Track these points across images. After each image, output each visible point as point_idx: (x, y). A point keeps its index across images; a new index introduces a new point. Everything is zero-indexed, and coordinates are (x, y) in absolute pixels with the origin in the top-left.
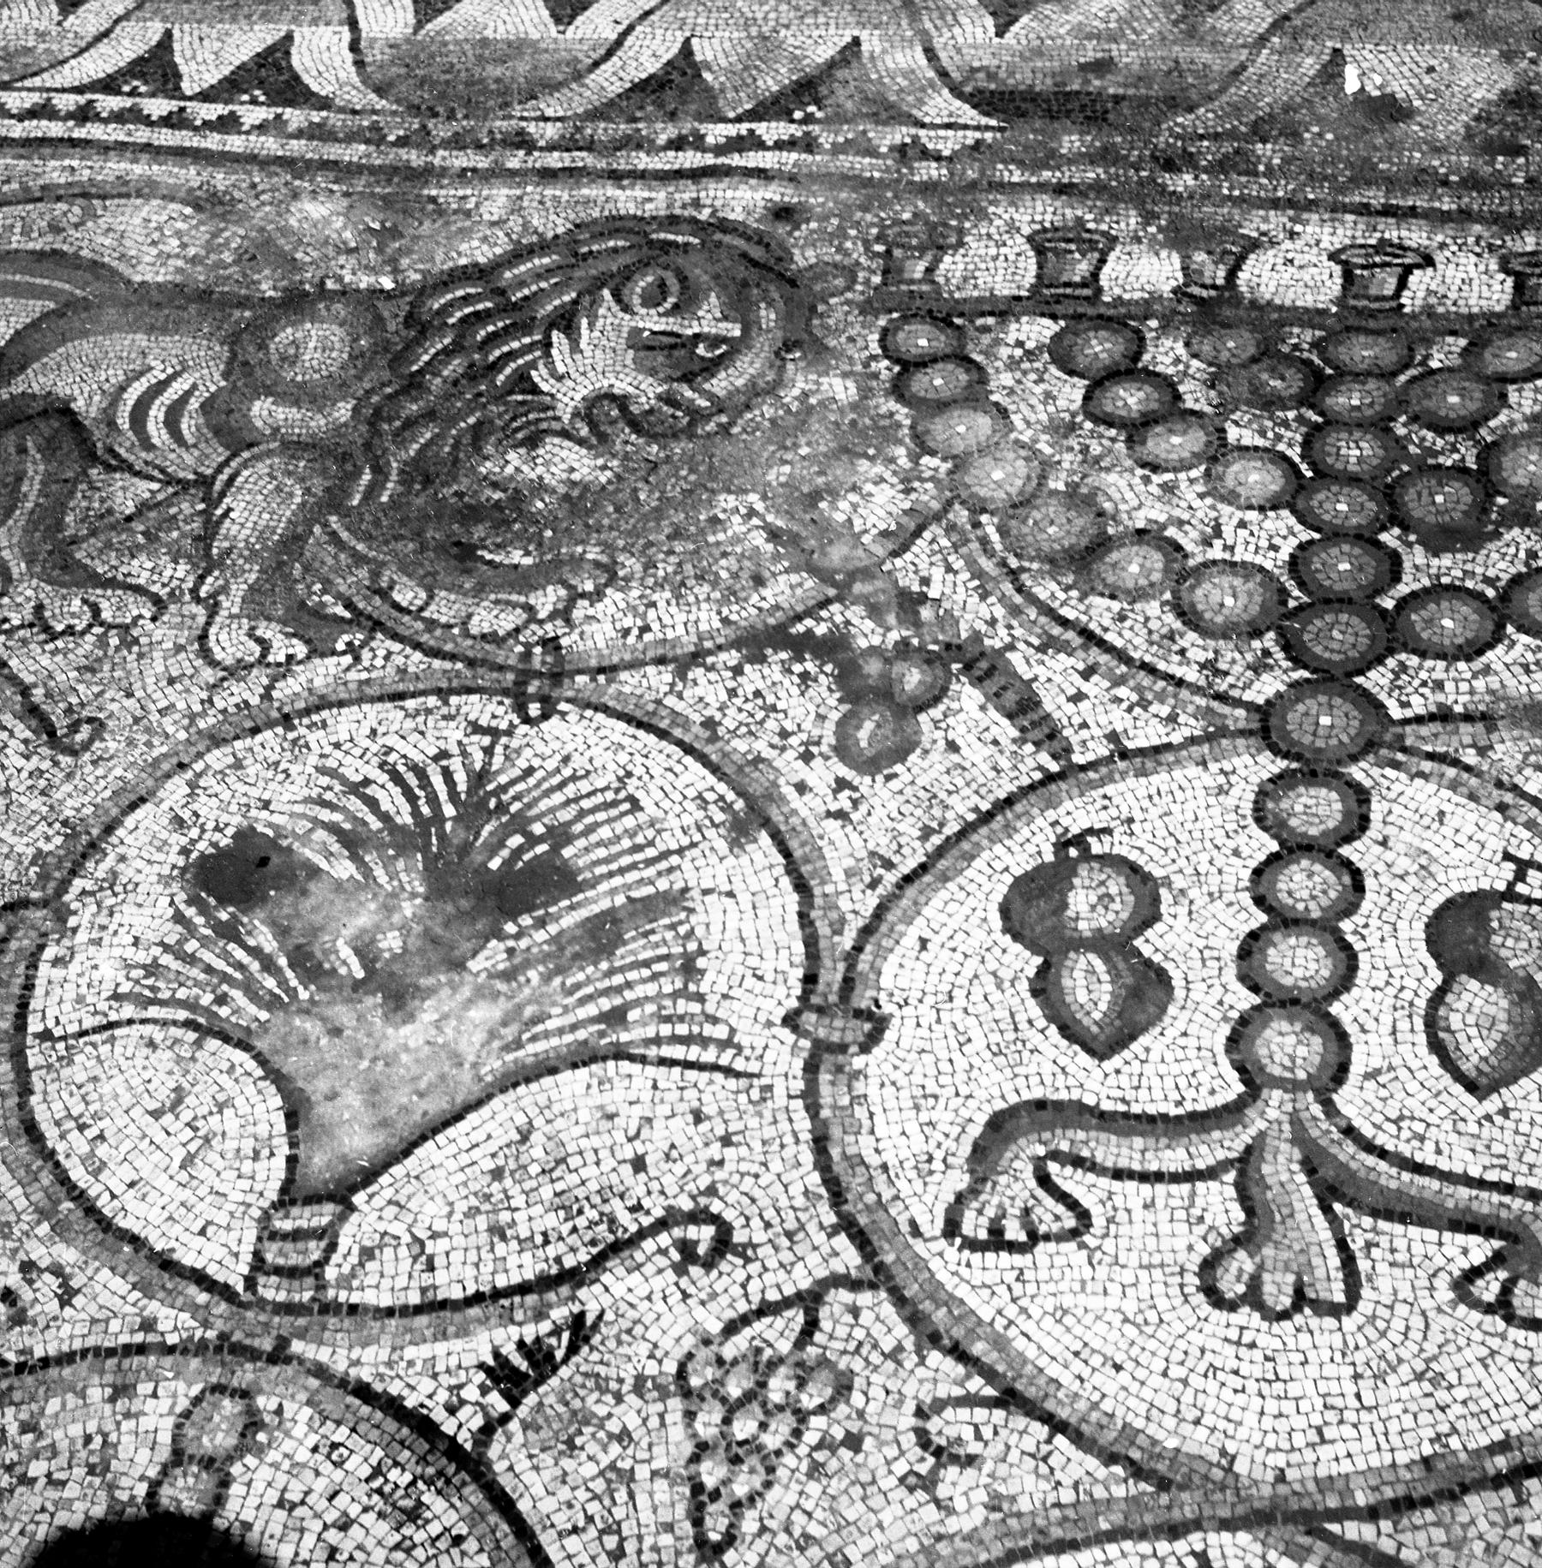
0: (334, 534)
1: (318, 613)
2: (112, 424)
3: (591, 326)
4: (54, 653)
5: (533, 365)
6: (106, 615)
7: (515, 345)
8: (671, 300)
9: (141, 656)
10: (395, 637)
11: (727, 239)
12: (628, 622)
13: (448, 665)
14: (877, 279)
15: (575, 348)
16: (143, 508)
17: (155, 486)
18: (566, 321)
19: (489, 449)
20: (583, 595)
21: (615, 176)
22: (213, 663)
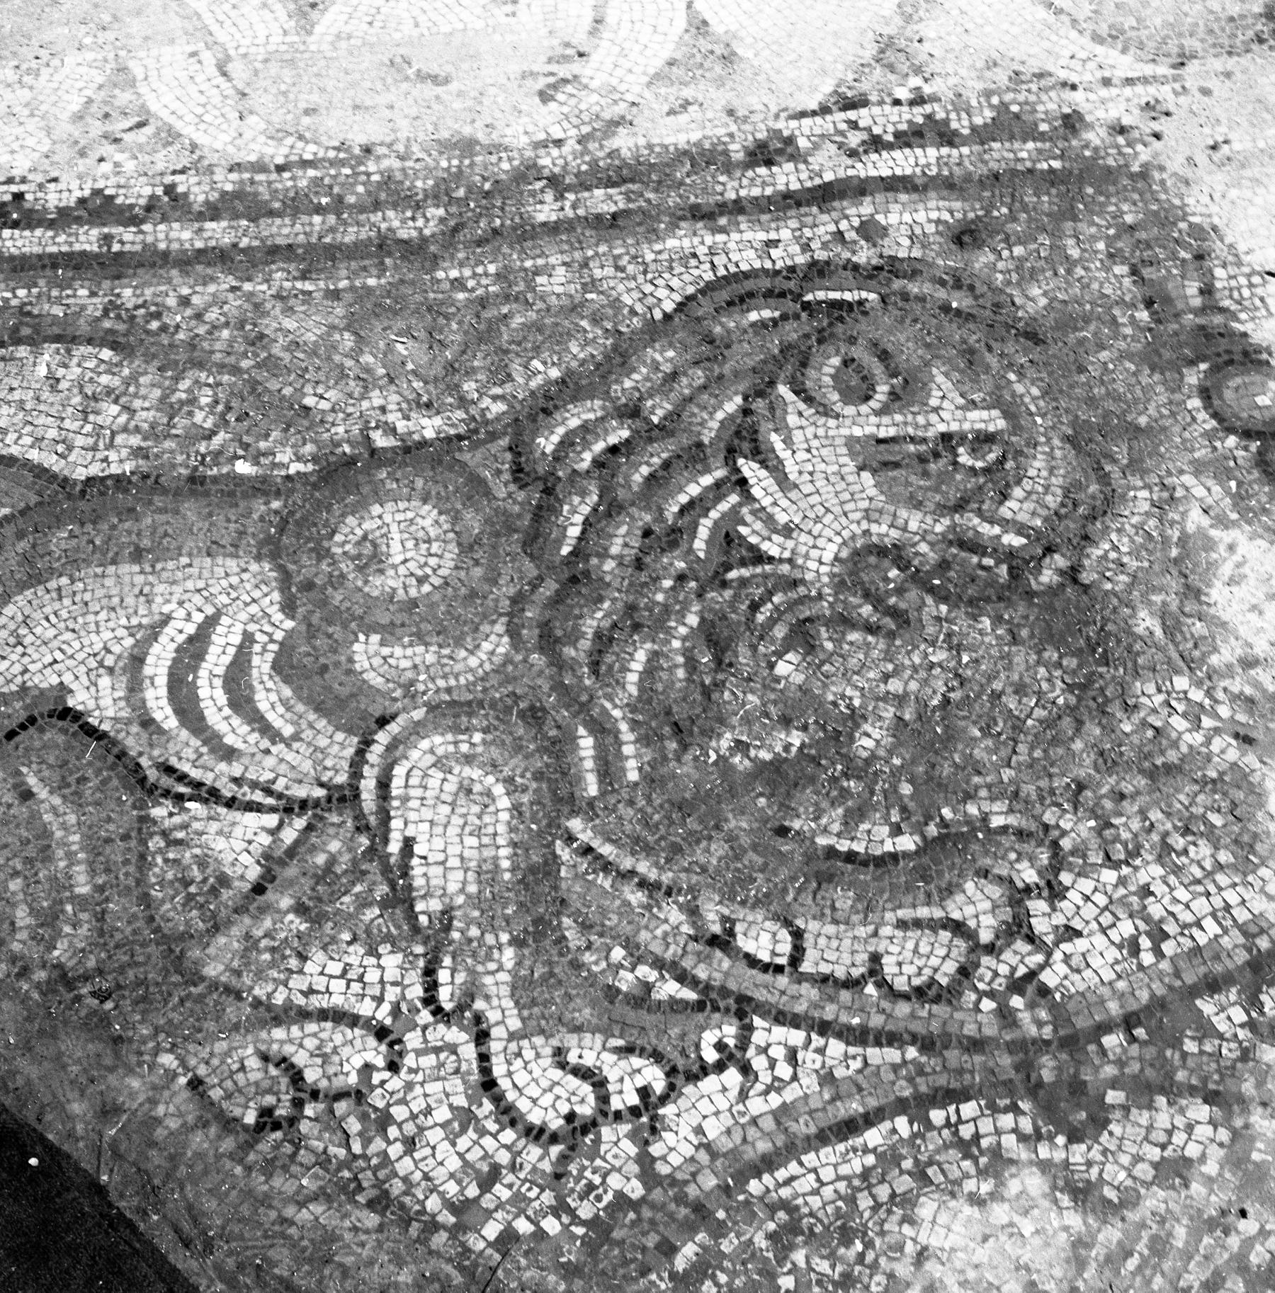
0: (587, 850)
1: (642, 997)
2: (147, 723)
3: (788, 442)
4: (269, 1167)
6: (311, 1076)
7: (694, 490)
8: (883, 389)
9: (410, 1144)
10: (781, 1018)
12: (1126, 928)
13: (893, 1055)
14: (1143, 315)
15: (783, 482)
16: (272, 863)
17: (272, 820)
18: (745, 439)
21: (702, 215)
22: (536, 1134)
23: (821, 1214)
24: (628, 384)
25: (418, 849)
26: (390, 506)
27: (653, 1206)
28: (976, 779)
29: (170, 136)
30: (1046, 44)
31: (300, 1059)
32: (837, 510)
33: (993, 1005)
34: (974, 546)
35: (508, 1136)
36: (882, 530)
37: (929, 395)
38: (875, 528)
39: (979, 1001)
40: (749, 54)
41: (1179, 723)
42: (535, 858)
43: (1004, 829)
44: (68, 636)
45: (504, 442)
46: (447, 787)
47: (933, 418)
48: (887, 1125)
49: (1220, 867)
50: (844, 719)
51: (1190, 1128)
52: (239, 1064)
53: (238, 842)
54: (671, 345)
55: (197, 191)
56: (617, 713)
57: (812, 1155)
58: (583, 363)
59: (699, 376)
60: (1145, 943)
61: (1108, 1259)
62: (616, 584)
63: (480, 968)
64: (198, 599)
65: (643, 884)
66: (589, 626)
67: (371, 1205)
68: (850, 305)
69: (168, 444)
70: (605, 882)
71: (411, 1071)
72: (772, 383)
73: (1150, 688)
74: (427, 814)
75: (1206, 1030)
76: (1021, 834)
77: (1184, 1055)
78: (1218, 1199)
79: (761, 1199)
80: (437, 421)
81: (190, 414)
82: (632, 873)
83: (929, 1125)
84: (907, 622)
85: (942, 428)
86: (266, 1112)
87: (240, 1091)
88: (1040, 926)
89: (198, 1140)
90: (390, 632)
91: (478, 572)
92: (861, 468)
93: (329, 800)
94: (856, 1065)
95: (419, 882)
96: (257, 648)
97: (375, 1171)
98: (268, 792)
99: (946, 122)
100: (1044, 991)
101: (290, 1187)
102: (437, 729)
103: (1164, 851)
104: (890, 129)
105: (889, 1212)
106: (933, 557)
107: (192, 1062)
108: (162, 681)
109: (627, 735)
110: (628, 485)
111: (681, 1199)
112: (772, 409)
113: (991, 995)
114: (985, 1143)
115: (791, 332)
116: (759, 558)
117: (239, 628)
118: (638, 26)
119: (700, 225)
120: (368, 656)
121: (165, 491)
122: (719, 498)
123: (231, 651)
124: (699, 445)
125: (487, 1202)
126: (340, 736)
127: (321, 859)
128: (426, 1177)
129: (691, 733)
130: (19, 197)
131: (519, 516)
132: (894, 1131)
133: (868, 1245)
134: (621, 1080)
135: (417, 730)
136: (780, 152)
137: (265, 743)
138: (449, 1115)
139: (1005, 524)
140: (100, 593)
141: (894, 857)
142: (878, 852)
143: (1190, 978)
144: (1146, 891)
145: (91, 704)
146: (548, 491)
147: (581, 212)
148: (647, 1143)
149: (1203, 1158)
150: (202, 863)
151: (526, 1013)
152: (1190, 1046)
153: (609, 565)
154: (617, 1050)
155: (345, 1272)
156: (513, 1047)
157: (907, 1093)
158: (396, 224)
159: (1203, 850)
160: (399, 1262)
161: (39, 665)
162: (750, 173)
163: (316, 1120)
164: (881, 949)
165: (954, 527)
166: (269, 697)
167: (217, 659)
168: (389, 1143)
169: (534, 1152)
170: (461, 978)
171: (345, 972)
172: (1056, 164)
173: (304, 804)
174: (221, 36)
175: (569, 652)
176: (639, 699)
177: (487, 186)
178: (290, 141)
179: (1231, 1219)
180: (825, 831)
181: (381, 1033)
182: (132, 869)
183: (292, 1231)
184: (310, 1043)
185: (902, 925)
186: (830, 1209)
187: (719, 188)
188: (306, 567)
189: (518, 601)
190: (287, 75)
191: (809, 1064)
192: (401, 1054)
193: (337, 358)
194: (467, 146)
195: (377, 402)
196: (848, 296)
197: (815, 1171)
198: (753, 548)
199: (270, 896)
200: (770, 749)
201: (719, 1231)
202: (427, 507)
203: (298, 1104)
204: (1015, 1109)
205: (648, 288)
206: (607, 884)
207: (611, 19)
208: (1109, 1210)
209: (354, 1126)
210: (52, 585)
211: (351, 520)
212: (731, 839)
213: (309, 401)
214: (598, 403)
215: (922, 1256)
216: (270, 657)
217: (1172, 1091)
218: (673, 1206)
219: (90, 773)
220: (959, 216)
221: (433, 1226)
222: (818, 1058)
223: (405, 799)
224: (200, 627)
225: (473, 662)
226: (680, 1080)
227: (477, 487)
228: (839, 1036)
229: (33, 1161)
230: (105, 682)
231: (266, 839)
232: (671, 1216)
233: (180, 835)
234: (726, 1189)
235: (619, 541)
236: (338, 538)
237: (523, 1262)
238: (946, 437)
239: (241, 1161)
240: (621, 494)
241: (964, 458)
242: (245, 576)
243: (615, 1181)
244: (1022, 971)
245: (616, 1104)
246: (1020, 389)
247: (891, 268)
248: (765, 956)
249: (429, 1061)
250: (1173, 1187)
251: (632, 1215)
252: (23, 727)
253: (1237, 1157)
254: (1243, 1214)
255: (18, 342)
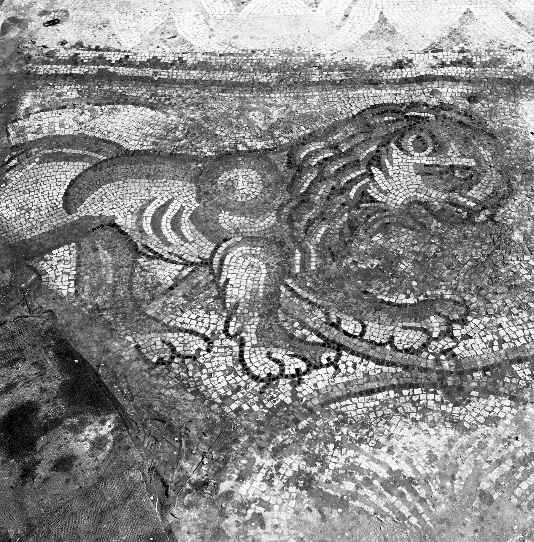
0: (292, 290)
1: (303, 340)
2: (142, 231)
3: (391, 162)
4: (158, 376)
5: (367, 186)
6: (178, 349)
7: (353, 176)
9: (210, 376)
10: (353, 353)
11: (448, 114)
12: (490, 337)
13: (393, 370)
15: (387, 176)
16: (177, 281)
17: (180, 267)
18: (376, 160)
19: (362, 235)
20: (454, 321)
22: (255, 378)
23: (355, 418)
24: (335, 137)
25: (230, 282)
26: (240, 170)
27: (294, 407)
28: (442, 283)
29: (183, 41)
30: (514, 36)
31: (175, 344)
32: (406, 187)
33: (434, 357)
34: (456, 204)
35: (246, 377)
36: (421, 196)
37: (448, 152)
38: (419, 195)
39: (428, 356)
40: (401, 31)
41: (523, 271)
42: (272, 290)
43: (449, 300)
44: (119, 200)
45: (286, 153)
46: (244, 263)
47: (448, 160)
48: (385, 393)
49: (529, 321)
50: (395, 258)
51: (502, 407)
52: (154, 342)
53: (166, 273)
54: (354, 126)
55: (190, 60)
56: (311, 247)
57: (356, 399)
58: (319, 129)
59: (362, 138)
60: (496, 343)
61: (461, 447)
62: (319, 204)
63: (245, 323)
64: (167, 193)
65: (310, 303)
66: (306, 217)
67: (192, 393)
68: (423, 117)
69: (165, 142)
70: (297, 301)
71: (214, 352)
72: (389, 142)
73: (514, 259)
74: (236, 271)
75: (514, 375)
76: (455, 302)
77: (504, 383)
78: (508, 433)
79: (334, 410)
80: (263, 143)
81: (175, 132)
82: (307, 299)
83: (402, 395)
84: (425, 228)
85: (451, 163)
86: (161, 359)
87: (153, 351)
88: (456, 333)
89: (135, 364)
90: (233, 211)
91: (268, 195)
92: (417, 174)
93: (202, 263)
94: (378, 371)
95: (229, 293)
96: (185, 211)
97: (196, 382)
98: (180, 258)
99: (472, 59)
100: (454, 355)
101: (165, 383)
102: (245, 244)
103: (510, 313)
104: (450, 60)
105: (381, 420)
106: (439, 207)
107: (138, 340)
108: (149, 219)
109: (313, 254)
110: (329, 171)
111: (305, 406)
112: (387, 151)
113: (433, 354)
114: (421, 402)
115: (399, 126)
116: (373, 200)
117: (180, 204)
118: (361, 18)
119: (372, 86)
120: (224, 219)
121: (161, 157)
122: (362, 179)
123: (176, 211)
124: (358, 161)
125: (234, 397)
126: (209, 243)
127: (195, 281)
128: (214, 386)
129: (337, 256)
130: (127, 57)
131: (287, 178)
132: (388, 395)
133: (371, 430)
134: (290, 365)
135: (237, 244)
136: (407, 64)
137: (182, 243)
138: (225, 368)
139: (469, 198)
140: (132, 187)
141: (406, 305)
142: (400, 303)
143: (511, 357)
144: (500, 326)
145: (123, 223)
146: (299, 171)
147: (328, 78)
148: (296, 387)
149: (505, 419)
150: (153, 278)
151: (259, 339)
152: (507, 380)
153: (317, 198)
154: (291, 356)
155: (179, 412)
156: (253, 350)
157: (395, 383)
158: (259, 77)
159: (525, 315)
160: (198, 411)
161: (107, 209)
162: (393, 71)
163: (178, 363)
164: (395, 335)
165: (449, 198)
166: (187, 229)
167: (170, 213)
168: (202, 374)
169: (254, 384)
170: (238, 325)
171: (197, 318)
172: (511, 77)
173: (192, 264)
174: (208, 10)
175: (297, 225)
176: (320, 243)
177: (295, 67)
178: (226, 46)
179: (512, 440)
180: (381, 294)
181: (206, 339)
182: (127, 277)
183: (163, 397)
184: (180, 339)
185: (404, 328)
186: (359, 416)
187: (381, 75)
188: (207, 186)
189: (282, 206)
190: (229, 25)
191: (360, 369)
192: (212, 347)
193: (230, 119)
194: (290, 53)
195: (242, 135)
196: (423, 115)
197: (356, 404)
198: (371, 197)
199: (175, 291)
200: (366, 265)
201: (317, 418)
202: (254, 172)
203: (172, 358)
204: (435, 393)
205: (348, 106)
206: (297, 301)
207: (351, 15)
208: (465, 431)
209: (191, 367)
210: (117, 183)
211: (226, 173)
212: (345, 293)
213: (218, 132)
214: (322, 143)
215: (390, 437)
216: (189, 215)
217: (497, 394)
218: (301, 408)
219: (119, 245)
220: (470, 91)
221: (213, 402)
222: (365, 368)
223: (229, 266)
224: (166, 202)
225: (262, 224)
226: (312, 368)
227: (273, 168)
228: (373, 361)
229: (76, 361)
230: (129, 216)
231: (177, 273)
232: (300, 411)
233: (147, 268)
234: (322, 405)
235: (322, 190)
236: (220, 178)
237: (243, 418)
238: (452, 166)
239: (149, 373)
240: (326, 174)
241: (457, 174)
242: (185, 188)
243: (281, 397)
244: (446, 347)
245: (287, 372)
246: (483, 152)
247: (442, 106)
248: (351, 332)
249: (222, 350)
250: (491, 426)
251: (285, 409)
252: (98, 228)
253: (518, 420)
254: (517, 439)
255: (119, 104)
